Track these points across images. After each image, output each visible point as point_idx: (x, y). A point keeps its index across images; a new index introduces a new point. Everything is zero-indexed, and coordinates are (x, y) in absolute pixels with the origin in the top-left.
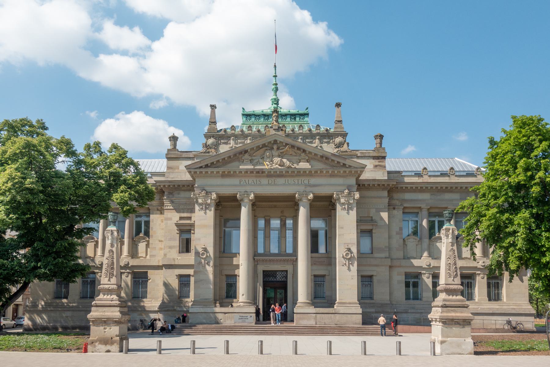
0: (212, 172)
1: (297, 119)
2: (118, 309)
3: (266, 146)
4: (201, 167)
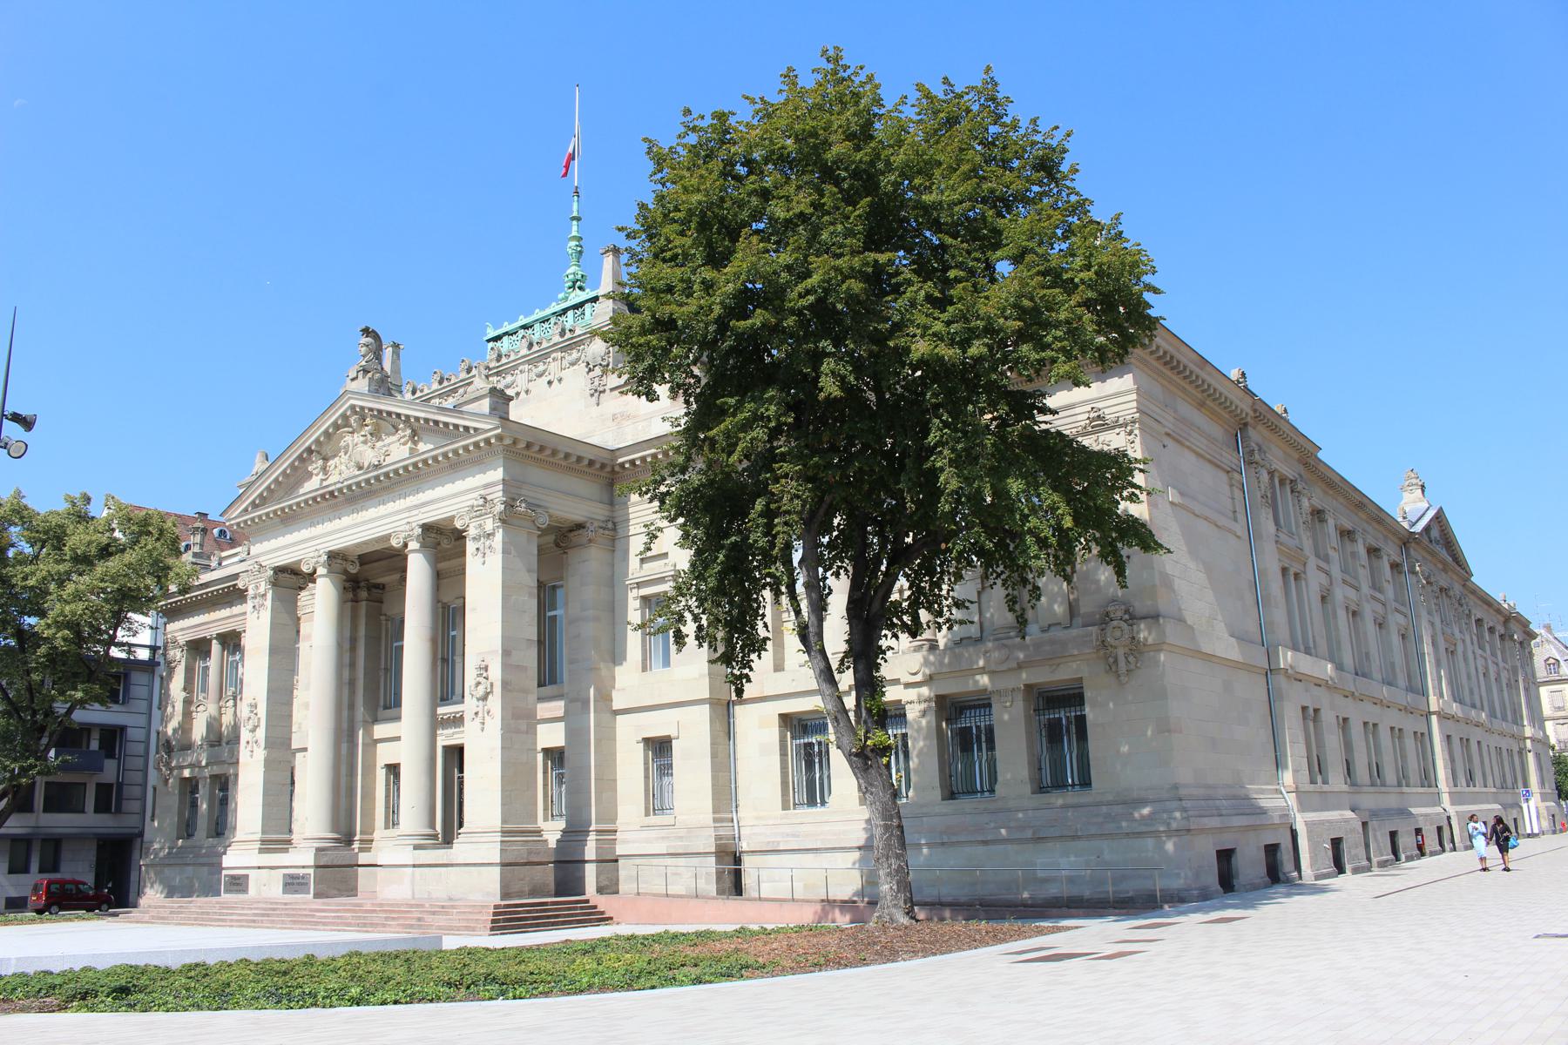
4: (246, 510)
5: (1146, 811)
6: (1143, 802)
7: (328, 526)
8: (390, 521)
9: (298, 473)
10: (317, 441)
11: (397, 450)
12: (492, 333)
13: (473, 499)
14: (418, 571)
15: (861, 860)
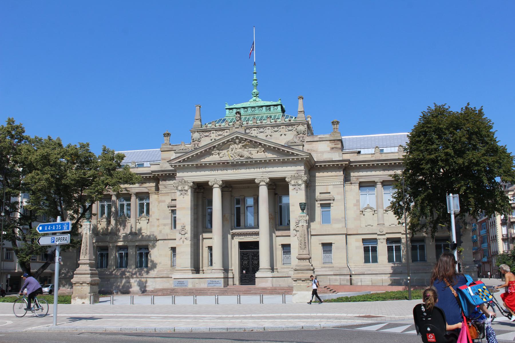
0: (188, 165)
1: (272, 108)
2: (89, 276)
3: (231, 142)
4: (180, 162)
5: (468, 267)
6: (467, 265)
7: (220, 172)
8: (261, 175)
9: (208, 152)
10: (219, 145)
11: (258, 154)
12: (228, 107)
13: (293, 173)
14: (263, 192)
15: (390, 277)
